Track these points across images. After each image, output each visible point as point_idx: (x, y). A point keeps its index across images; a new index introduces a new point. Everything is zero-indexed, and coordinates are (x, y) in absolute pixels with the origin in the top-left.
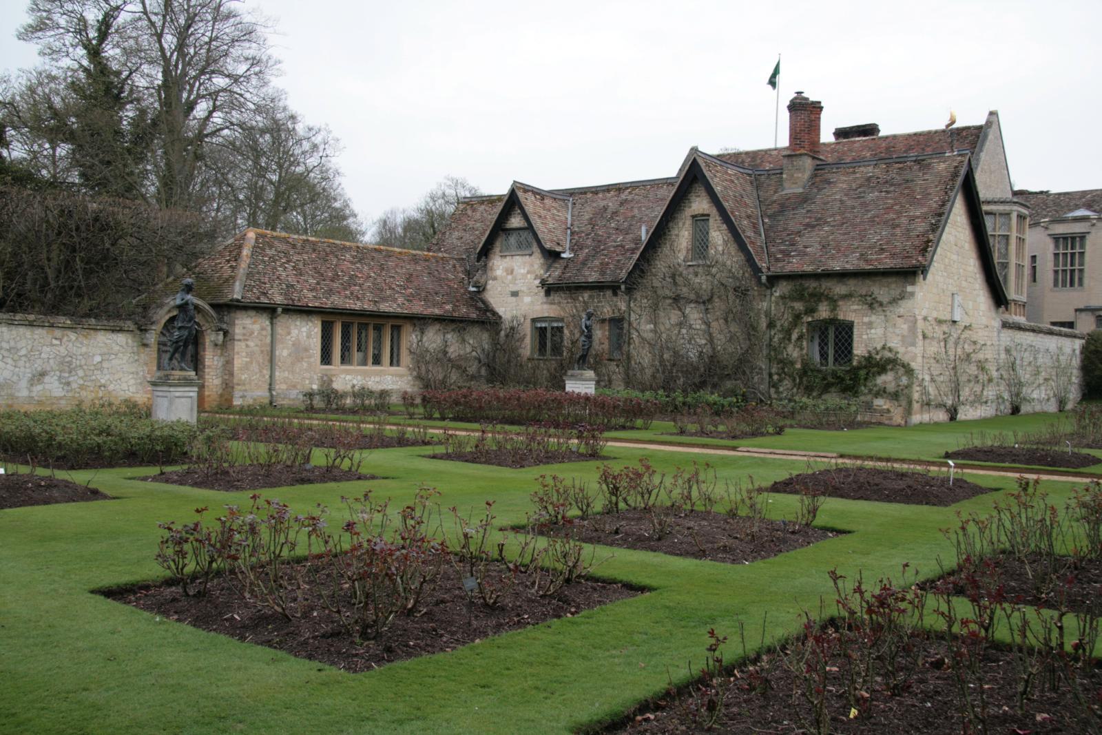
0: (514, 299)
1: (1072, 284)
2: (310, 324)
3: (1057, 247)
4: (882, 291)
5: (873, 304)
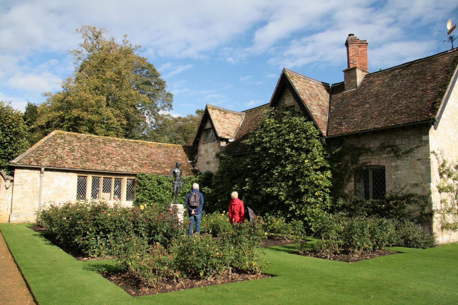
0: (207, 165)
2: (68, 177)
5: (396, 153)
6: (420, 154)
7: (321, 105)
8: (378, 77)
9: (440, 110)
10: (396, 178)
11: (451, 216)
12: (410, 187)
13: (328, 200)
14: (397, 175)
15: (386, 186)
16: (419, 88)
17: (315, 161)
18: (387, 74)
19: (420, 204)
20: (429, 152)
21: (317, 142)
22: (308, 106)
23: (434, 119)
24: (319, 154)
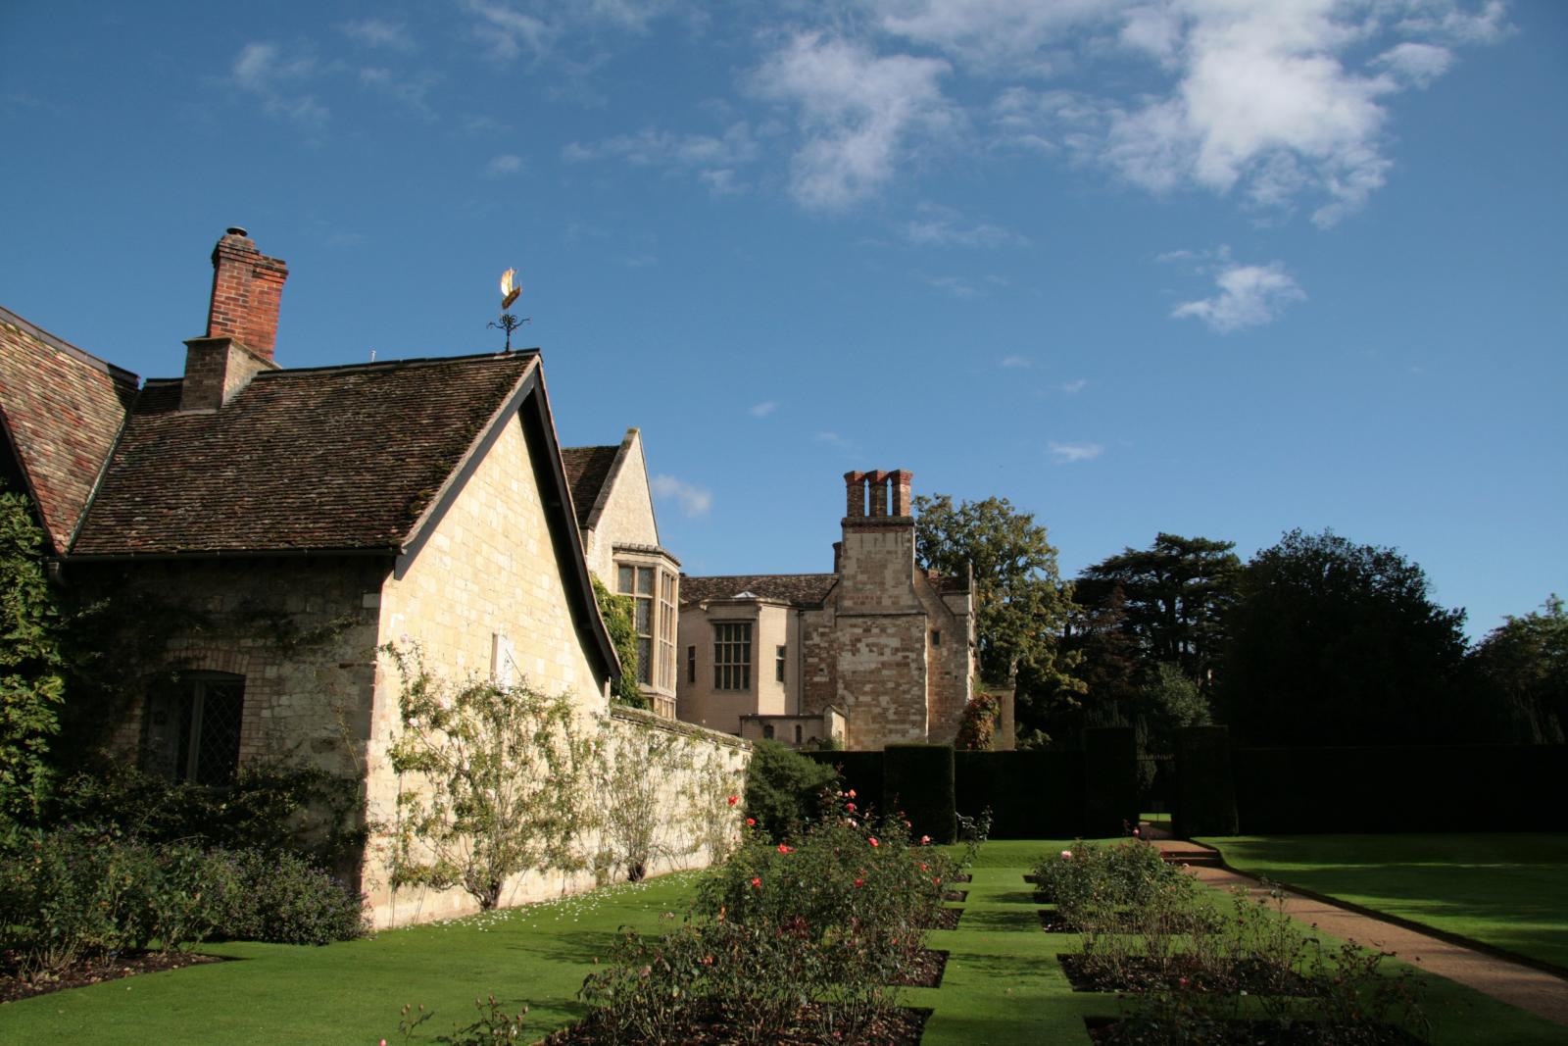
1: (737, 686)
3: (719, 636)
4: (303, 610)
5: (287, 641)
6: (349, 650)
7: (79, 443)
8: (292, 386)
9: (421, 522)
10: (273, 717)
11: (429, 842)
12: (310, 752)
13: (37, 781)
14: (277, 709)
15: (242, 741)
16: (391, 446)
17: (7, 637)
18: (322, 384)
19: (333, 805)
20: (375, 644)
21: (29, 571)
22: (19, 438)
23: (397, 547)
24: (28, 615)
